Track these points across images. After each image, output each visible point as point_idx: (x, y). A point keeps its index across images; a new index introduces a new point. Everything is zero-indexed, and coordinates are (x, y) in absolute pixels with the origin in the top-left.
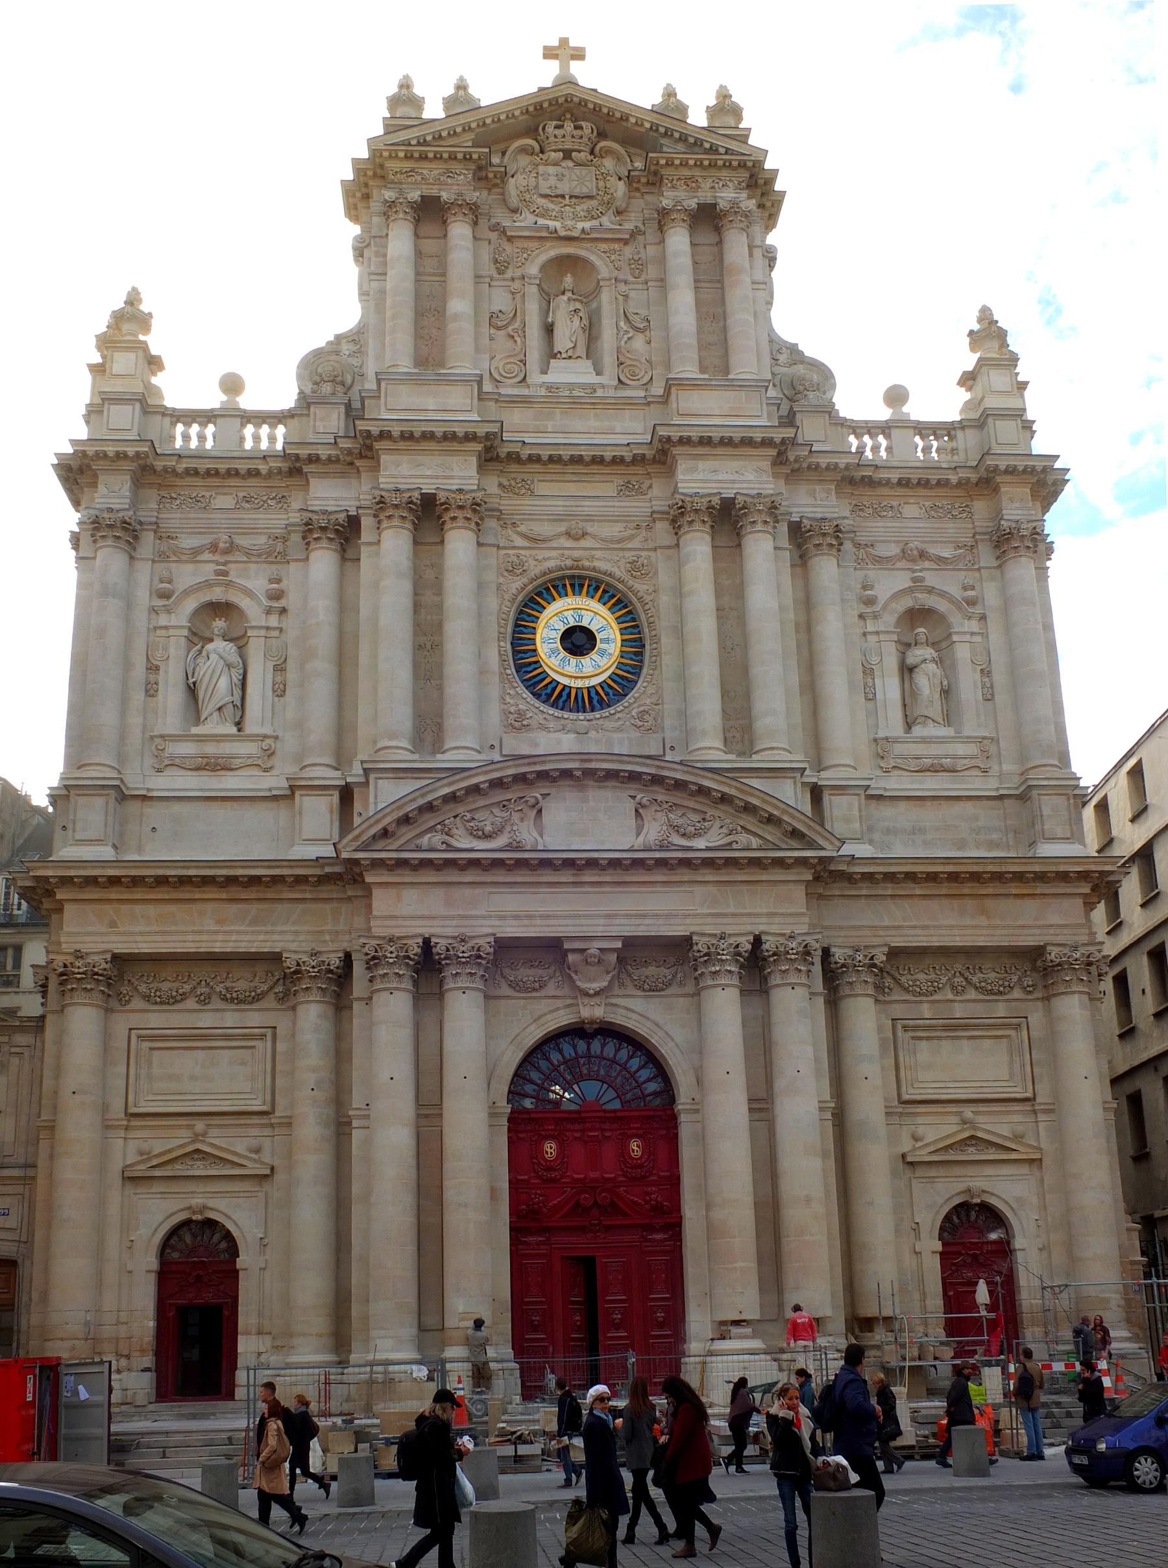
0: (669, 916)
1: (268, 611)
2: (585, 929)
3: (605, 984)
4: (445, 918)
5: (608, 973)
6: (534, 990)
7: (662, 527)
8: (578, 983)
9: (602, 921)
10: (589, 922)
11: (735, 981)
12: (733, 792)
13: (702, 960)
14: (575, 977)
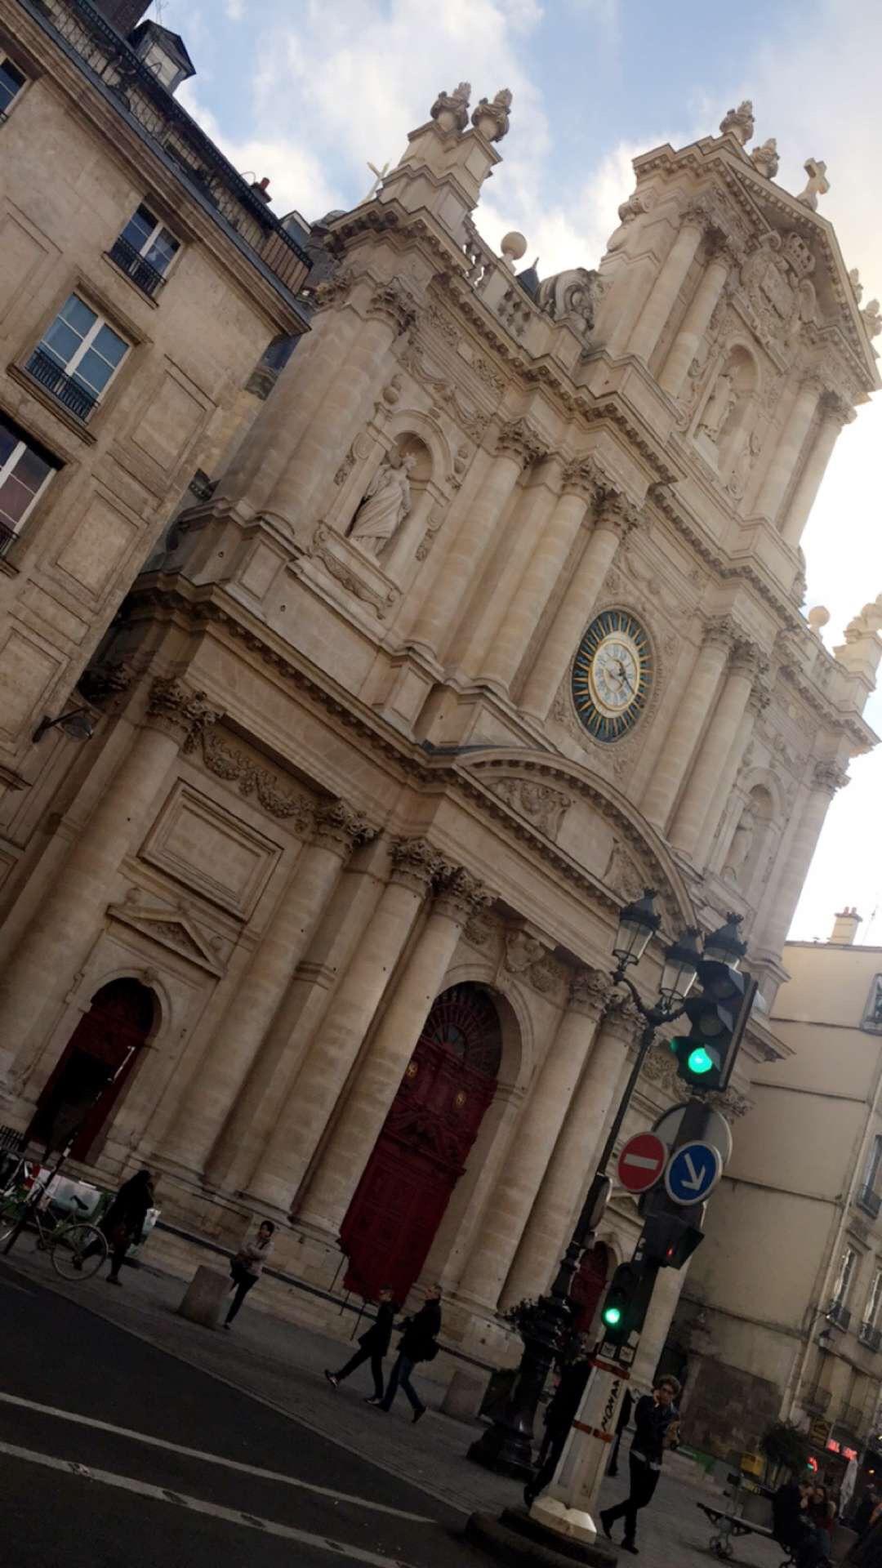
0: (591, 946)
1: (448, 480)
7: (697, 624)
12: (672, 880)
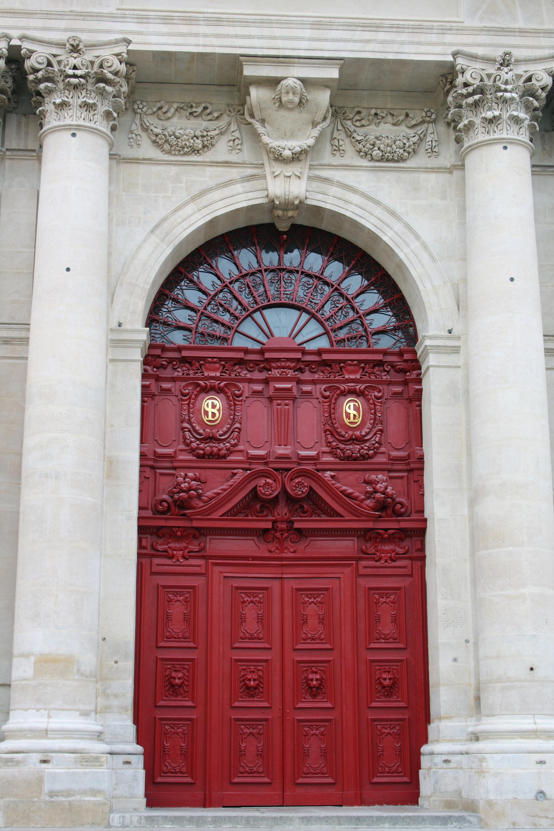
0: (418, 28)
2: (280, 43)
3: (311, 142)
4: (48, 15)
5: (314, 124)
6: (195, 151)
8: (266, 139)
9: (308, 33)
10: (286, 33)
11: (525, 138)
13: (470, 100)
14: (260, 129)
